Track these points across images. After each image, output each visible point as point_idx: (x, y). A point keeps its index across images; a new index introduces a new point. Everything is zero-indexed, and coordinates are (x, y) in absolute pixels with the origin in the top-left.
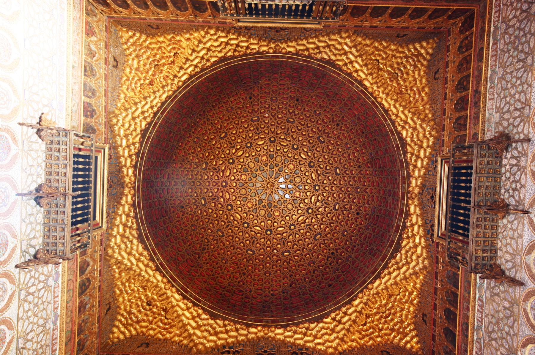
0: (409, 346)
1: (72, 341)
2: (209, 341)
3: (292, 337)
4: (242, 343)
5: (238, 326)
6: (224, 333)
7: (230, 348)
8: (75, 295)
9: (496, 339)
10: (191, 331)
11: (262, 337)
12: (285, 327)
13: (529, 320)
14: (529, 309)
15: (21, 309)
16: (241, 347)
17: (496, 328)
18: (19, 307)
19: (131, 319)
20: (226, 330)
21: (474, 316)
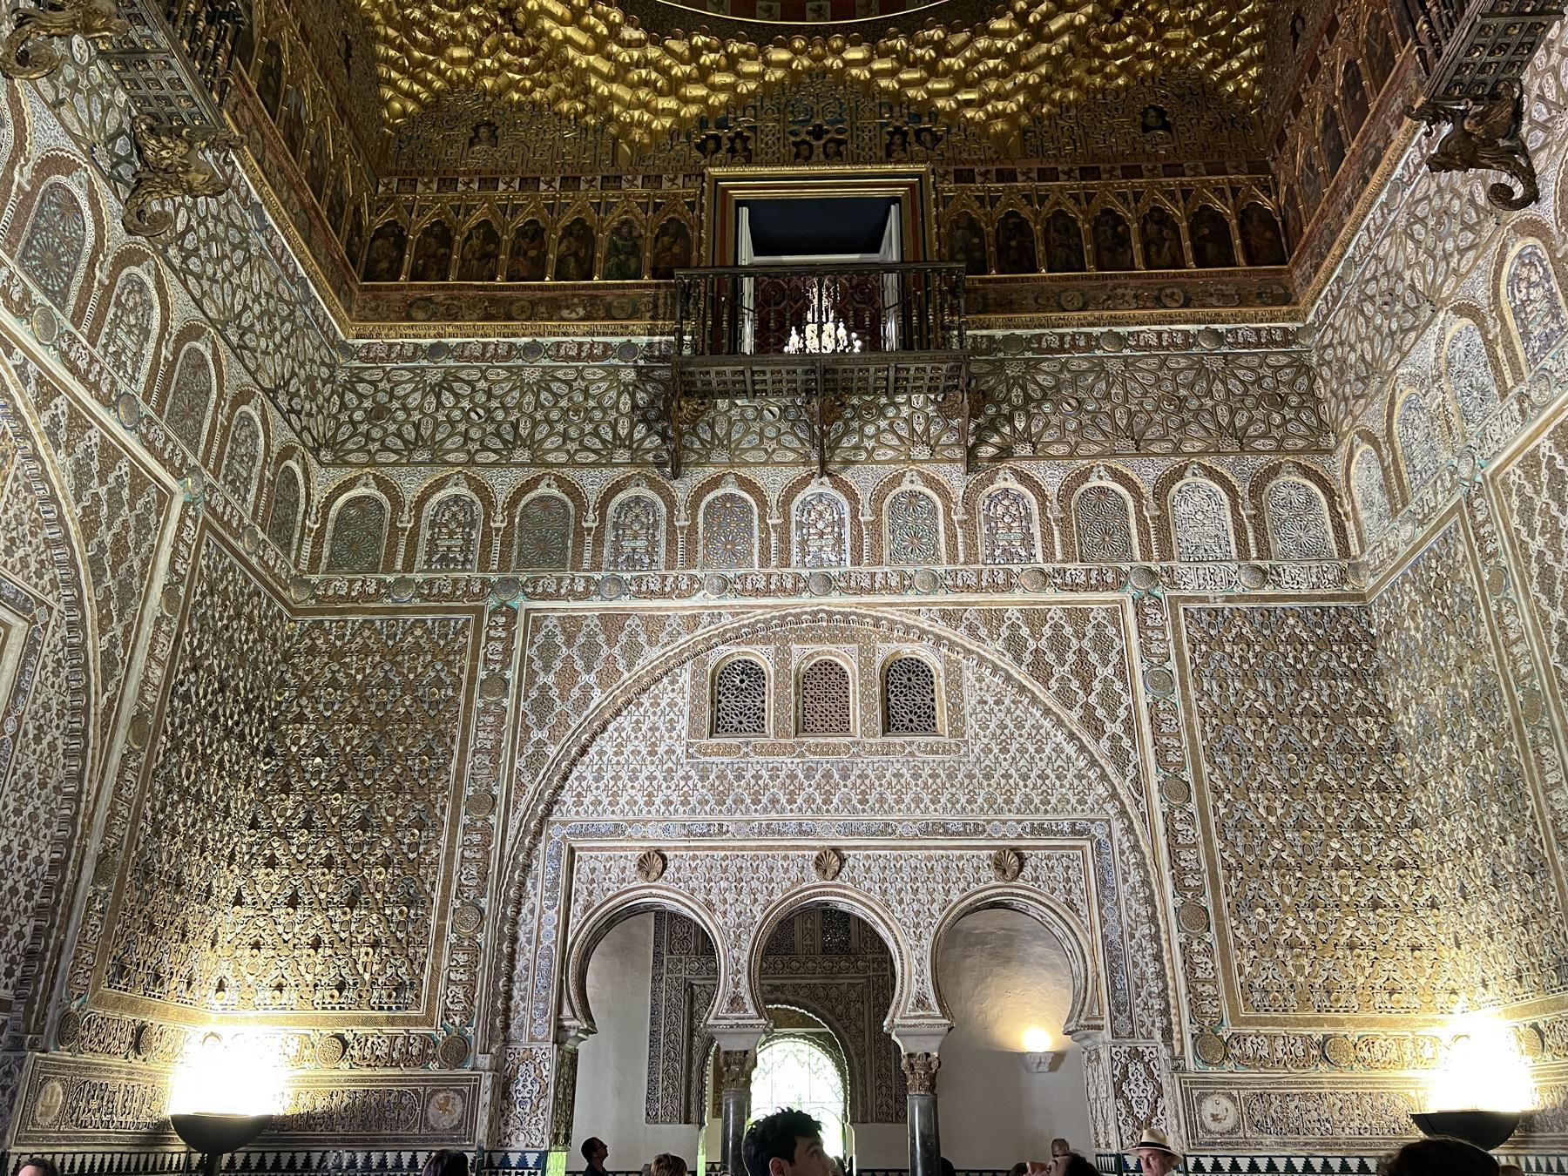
0: (1231, 89)
1: (317, 223)
2: (657, 113)
3: (892, 73)
4: (751, 101)
5: (735, 47)
6: (695, 81)
7: (721, 124)
8: (267, 131)
9: (1419, 242)
10: (604, 90)
11: (808, 71)
12: (871, 36)
13: (1497, 275)
14: (1512, 253)
15: (191, 281)
16: (746, 120)
17: (1431, 223)
18: (185, 283)
19: (414, 41)
20: (701, 67)
21: (1404, 150)
